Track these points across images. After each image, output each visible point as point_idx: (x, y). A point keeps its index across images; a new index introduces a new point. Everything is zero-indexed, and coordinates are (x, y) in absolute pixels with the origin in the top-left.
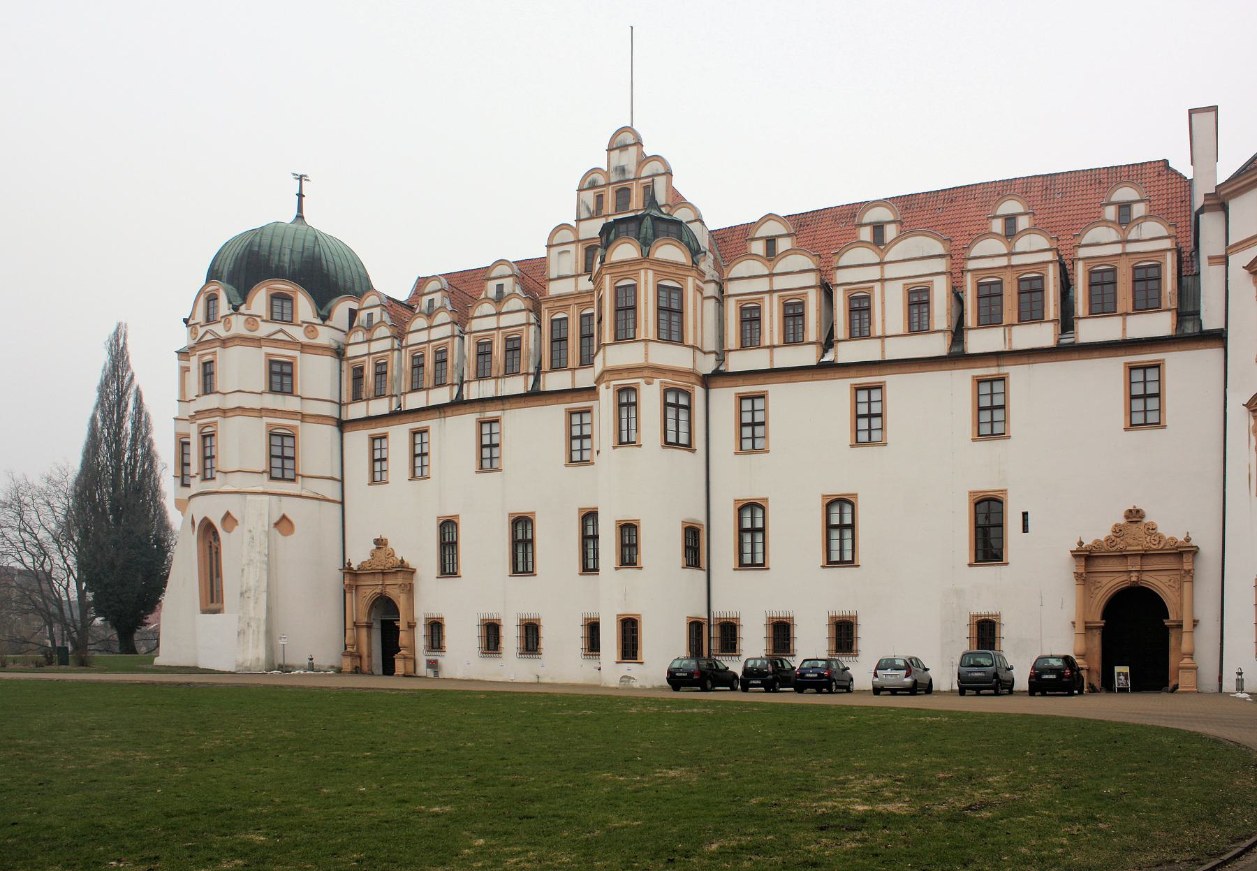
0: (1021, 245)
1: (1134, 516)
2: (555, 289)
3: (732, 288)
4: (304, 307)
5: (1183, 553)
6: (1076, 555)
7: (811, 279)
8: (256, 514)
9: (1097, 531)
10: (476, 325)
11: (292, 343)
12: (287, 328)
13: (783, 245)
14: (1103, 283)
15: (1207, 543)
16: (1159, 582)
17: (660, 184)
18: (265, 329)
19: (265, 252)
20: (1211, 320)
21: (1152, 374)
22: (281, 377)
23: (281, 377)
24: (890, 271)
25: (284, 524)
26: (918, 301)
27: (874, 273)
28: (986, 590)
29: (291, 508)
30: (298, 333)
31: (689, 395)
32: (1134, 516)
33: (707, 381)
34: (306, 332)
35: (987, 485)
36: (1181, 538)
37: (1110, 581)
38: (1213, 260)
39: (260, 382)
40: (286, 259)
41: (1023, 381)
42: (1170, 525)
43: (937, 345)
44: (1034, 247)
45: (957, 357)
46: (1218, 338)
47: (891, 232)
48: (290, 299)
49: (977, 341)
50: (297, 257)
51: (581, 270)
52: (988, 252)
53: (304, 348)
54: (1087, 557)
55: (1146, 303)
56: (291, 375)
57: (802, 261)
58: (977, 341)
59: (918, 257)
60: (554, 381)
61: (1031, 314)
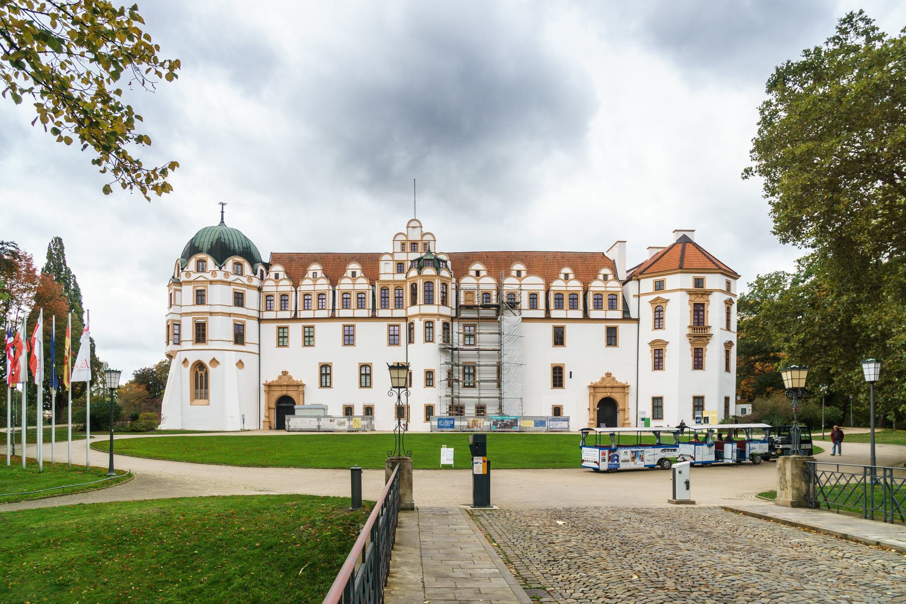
0: (570, 284)
1: (609, 375)
2: (382, 278)
3: (462, 286)
4: (247, 268)
5: (624, 388)
6: (590, 387)
7: (494, 287)
8: (228, 359)
9: (597, 380)
10: (342, 287)
11: (243, 285)
12: (240, 277)
13: (483, 273)
14: (598, 298)
15: (632, 384)
16: (616, 396)
17: (432, 244)
18: (232, 278)
19: (227, 242)
20: (633, 315)
21: (396, 328)
22: (239, 299)
23: (239, 299)
24: (523, 287)
25: (240, 364)
26: (533, 297)
27: (517, 287)
28: (557, 397)
29: (245, 358)
30: (245, 280)
31: (448, 324)
32: (609, 375)
33: (452, 319)
34: (248, 279)
35: (558, 362)
36: (624, 382)
37: (600, 396)
38: (634, 296)
39: (230, 300)
40: (236, 246)
41: (571, 330)
42: (621, 379)
43: (542, 314)
44: (575, 285)
45: (548, 318)
46: (637, 320)
47: (523, 274)
48: (241, 265)
49: (555, 314)
50: (241, 246)
51: (395, 271)
52: (558, 285)
53: (249, 287)
54: (594, 388)
55: (612, 307)
56: (242, 299)
57: (491, 280)
58: (555, 314)
59: (535, 283)
60: (381, 313)
61: (574, 307)
